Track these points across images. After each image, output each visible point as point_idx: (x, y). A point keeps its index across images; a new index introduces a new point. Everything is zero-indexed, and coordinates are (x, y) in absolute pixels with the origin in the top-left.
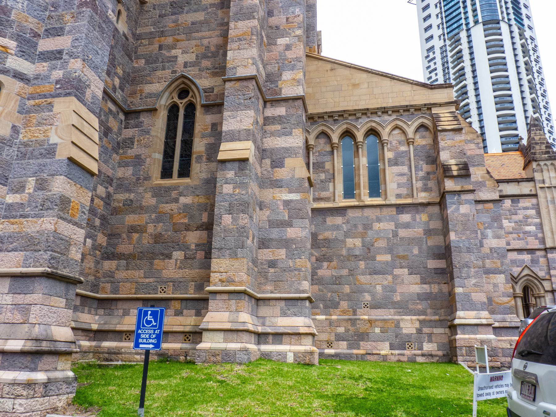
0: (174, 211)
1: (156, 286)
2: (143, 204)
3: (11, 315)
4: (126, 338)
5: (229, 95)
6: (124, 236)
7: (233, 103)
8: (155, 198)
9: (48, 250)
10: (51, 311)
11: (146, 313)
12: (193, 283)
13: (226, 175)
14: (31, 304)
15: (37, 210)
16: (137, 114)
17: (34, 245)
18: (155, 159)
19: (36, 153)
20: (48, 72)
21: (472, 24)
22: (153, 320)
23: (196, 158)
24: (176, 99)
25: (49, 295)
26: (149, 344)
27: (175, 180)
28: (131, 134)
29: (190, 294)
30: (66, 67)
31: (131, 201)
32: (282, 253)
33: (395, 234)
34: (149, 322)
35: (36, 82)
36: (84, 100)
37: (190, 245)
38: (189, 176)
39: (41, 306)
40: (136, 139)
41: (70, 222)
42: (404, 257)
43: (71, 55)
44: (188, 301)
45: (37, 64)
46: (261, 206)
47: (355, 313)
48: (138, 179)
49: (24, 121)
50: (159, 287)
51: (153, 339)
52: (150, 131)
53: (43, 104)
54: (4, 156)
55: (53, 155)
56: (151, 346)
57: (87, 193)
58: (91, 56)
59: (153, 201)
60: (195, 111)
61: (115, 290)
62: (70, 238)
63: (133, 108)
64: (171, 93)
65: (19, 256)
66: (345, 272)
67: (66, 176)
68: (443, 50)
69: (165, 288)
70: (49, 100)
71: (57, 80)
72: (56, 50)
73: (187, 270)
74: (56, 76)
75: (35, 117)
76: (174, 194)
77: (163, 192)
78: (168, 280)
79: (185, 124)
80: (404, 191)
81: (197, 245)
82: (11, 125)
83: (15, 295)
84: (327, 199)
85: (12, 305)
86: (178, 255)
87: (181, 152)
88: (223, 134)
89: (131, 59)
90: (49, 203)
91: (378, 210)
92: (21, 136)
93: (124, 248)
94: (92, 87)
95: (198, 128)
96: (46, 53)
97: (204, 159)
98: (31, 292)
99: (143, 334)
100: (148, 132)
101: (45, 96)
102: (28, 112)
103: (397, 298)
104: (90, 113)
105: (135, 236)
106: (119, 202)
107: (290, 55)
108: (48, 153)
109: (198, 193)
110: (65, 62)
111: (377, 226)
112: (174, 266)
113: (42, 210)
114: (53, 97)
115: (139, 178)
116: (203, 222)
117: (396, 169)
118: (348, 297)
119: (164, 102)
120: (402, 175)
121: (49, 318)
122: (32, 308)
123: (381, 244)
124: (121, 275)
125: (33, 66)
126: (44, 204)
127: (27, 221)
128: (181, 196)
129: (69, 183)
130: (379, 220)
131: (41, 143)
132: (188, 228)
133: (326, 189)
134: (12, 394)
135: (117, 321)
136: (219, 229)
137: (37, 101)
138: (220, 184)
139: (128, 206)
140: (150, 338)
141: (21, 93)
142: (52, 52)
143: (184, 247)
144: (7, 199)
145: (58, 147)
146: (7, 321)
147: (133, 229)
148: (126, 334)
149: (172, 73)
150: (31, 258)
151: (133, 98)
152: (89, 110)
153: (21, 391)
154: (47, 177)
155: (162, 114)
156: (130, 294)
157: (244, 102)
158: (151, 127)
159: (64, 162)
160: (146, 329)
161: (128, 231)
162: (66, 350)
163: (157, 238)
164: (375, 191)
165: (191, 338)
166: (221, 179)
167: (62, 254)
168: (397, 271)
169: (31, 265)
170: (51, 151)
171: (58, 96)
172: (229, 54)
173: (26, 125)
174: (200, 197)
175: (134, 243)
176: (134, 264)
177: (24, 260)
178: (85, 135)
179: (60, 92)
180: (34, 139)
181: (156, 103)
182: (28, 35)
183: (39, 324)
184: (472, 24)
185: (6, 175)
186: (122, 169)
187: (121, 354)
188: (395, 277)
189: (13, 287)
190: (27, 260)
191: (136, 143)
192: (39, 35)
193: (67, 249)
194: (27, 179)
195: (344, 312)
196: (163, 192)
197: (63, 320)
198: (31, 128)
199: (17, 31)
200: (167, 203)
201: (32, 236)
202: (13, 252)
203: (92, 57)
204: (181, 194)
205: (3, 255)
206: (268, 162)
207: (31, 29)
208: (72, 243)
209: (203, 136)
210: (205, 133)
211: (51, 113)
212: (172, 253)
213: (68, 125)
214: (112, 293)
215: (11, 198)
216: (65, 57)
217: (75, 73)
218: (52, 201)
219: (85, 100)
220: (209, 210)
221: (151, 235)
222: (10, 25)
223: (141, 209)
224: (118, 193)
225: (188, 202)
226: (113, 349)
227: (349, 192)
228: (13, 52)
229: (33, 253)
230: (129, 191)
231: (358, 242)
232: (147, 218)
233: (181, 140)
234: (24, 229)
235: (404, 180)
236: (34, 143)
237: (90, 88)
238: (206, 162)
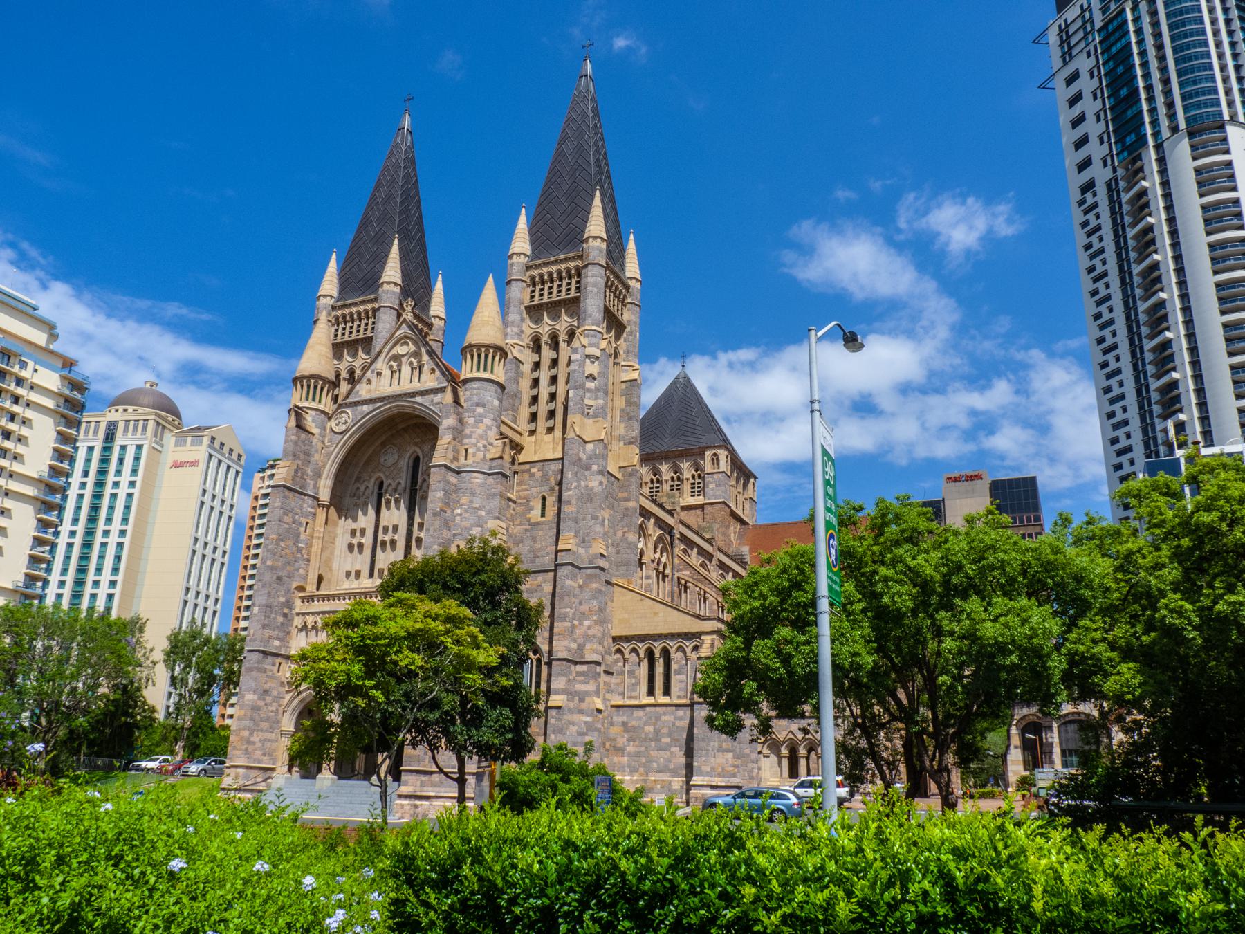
21: (1166, 133)
33: (674, 724)
42: (677, 740)
46: (573, 724)
47: (647, 775)
66: (643, 749)
68: (1112, 187)
80: (682, 694)
84: (635, 698)
91: (664, 708)
103: (672, 766)
107: (590, 633)
111: (663, 718)
117: (678, 677)
118: (644, 765)
120: (682, 682)
123: (665, 731)
130: (665, 714)
133: (635, 691)
164: (667, 692)
168: (673, 749)
184: (1166, 133)
188: (672, 753)
195: (641, 775)
206: (577, 699)
227: (651, 692)
231: (651, 729)
235: (683, 686)
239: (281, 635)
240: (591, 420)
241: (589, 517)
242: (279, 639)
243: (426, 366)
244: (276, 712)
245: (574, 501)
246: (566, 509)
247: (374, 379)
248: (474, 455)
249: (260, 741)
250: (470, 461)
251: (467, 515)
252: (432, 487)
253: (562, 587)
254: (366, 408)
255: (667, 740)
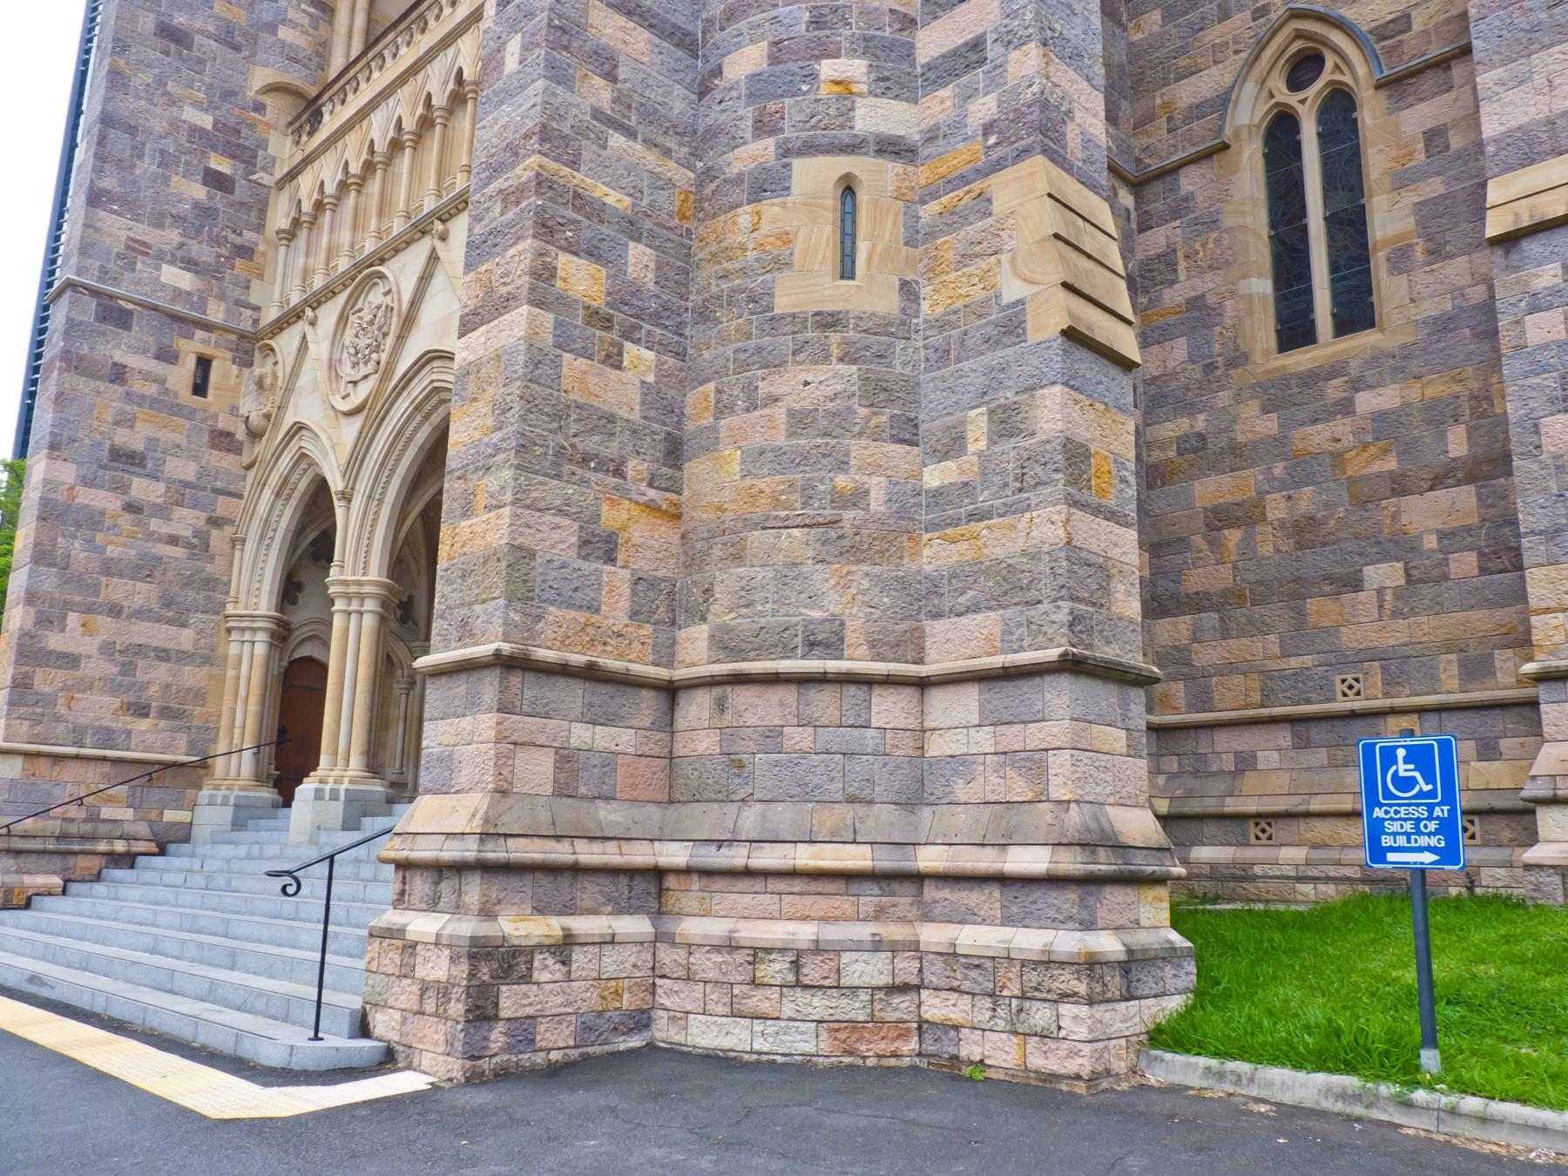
0: (1344, 442)
1: (1326, 678)
2: (1240, 439)
3: (998, 780)
4: (1260, 835)
5: (1485, 11)
6: (1198, 541)
7: (1504, 33)
8: (1274, 416)
9: (1062, 598)
10: (1097, 764)
11: (1389, 756)
12: (1453, 657)
13: (1527, 284)
14: (1046, 750)
15: (1009, 493)
16: (1170, 179)
17: (1022, 588)
18: (1250, 296)
19: (974, 340)
20: (958, 111)
22: (1417, 775)
23: (1388, 259)
24: (1284, 96)
25: (1086, 721)
26: (1421, 850)
27: (1327, 345)
28: (1162, 241)
29: (1449, 692)
30: (1002, 81)
31: (1201, 437)
34: (1405, 784)
35: (930, 149)
36: (1065, 159)
37: (1420, 537)
38: (1372, 325)
39: (1073, 752)
40: (1180, 254)
41: (1097, 511)
43: (1010, 41)
44: (1445, 715)
45: (924, 100)
48: (1210, 368)
49: (925, 262)
50: (1338, 679)
51: (1429, 834)
52: (1220, 217)
53: (963, 202)
54: (899, 369)
55: (1018, 336)
56: (1428, 858)
57: (1123, 424)
58: (1058, 27)
59: (1269, 425)
60: (1354, 109)
61: (1202, 700)
62: (1107, 559)
63: (1154, 164)
64: (1264, 82)
65: (987, 623)
67: (1066, 384)
69: (1357, 680)
70: (976, 186)
71: (984, 125)
72: (966, 44)
73: (1424, 619)
74: (979, 115)
75: (950, 245)
76: (1334, 390)
77: (1297, 390)
78: (1361, 656)
79: (1327, 162)
81: (1442, 536)
82: (897, 283)
83: (999, 728)
85: (996, 753)
86: (1384, 575)
87: (1330, 255)
88: (1490, 149)
89: (1119, 23)
90: (1038, 469)
92: (925, 306)
93: (1204, 577)
94: (1078, 115)
95: (1376, 162)
96: (940, 61)
97: (1419, 254)
98: (1039, 716)
99: (1391, 819)
100: (1213, 223)
101: (964, 180)
102: (931, 235)
104: (1086, 191)
105: (1233, 537)
106: (1163, 448)
108: (1005, 333)
109: (1416, 370)
110: (995, 68)
112: (1376, 611)
113: (1020, 490)
114: (984, 173)
115: (1211, 364)
116: (1454, 459)
119: (1249, 113)
121: (1098, 785)
122: (1051, 759)
124: (1208, 655)
125: (914, 109)
126: (1023, 474)
127: (989, 528)
128: (1357, 390)
129: (1076, 402)
131: (979, 310)
132: (1399, 486)
134: (1049, 991)
135: (1223, 786)
136: (1535, 467)
137: (944, 199)
138: (1511, 319)
139: (1195, 453)
140: (1419, 833)
141: (903, 190)
142: (955, 53)
143: (1399, 546)
144: (926, 478)
145: (1029, 307)
146: (993, 798)
147: (1220, 518)
148: (1257, 824)
149: (1254, 19)
150: (1019, 625)
151: (1149, 137)
152: (1082, 183)
153: (1072, 983)
154: (1016, 399)
155: (1246, 153)
156: (1247, 706)
157: (1551, 16)
158: (1218, 205)
159: (1055, 344)
160: (1400, 805)
161: (1207, 525)
162: (1154, 872)
163: (1303, 531)
165: (1476, 829)
166: (1513, 300)
167: (1094, 604)
169: (1025, 644)
170: (1012, 325)
171: (998, 166)
173: (933, 272)
174: (1425, 379)
175: (1233, 558)
176: (1243, 620)
177: (1003, 633)
178: (1090, 257)
179: (1000, 154)
180: (959, 304)
181: (1221, 129)
182: (888, 30)
183: (1077, 802)
185: (913, 415)
186: (1157, 348)
187: (1254, 878)
189: (990, 707)
190: (1012, 633)
191: (1182, 265)
192: (913, 21)
193: (1105, 589)
194: (965, 416)
196: (1297, 390)
197: (1128, 789)
198: (945, 278)
199: (860, 28)
200: (1315, 421)
201: (1009, 566)
202: (971, 616)
203: (1062, 26)
204: (1358, 384)
205: (948, 627)
207: (891, 10)
208: (1113, 571)
209: (1401, 181)
210: (1406, 171)
211: (990, 220)
212: (1361, 571)
213: (1043, 240)
214: (1193, 708)
215: (936, 473)
216: (993, 51)
217: (1031, 86)
218: (1043, 460)
219: (1068, 156)
220: (1467, 418)
221: (1283, 526)
222: (843, 19)
223: (1237, 455)
224: (1156, 423)
225: (1385, 407)
226: (1227, 866)
228: (863, 88)
229: (1021, 612)
230: (1188, 408)
232: (1260, 477)
233: (1326, 219)
234: (986, 551)
236: (961, 314)
237: (1073, 119)
238: (1429, 264)
239: (202, 251)
242: (190, 264)
244: (200, 546)
249: (107, 650)
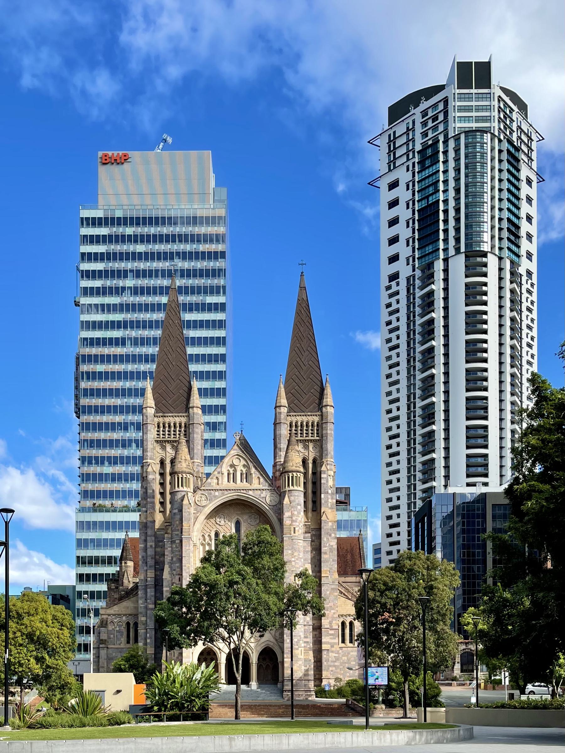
32: (334, 668)
111: (351, 653)
123: (352, 659)
130: (352, 652)
172: (323, 621)
227: (343, 641)
231: (346, 658)
240: (330, 510)
241: (331, 560)
243: (254, 475)
245: (328, 553)
246: (324, 556)
247: (220, 478)
248: (298, 531)
250: (297, 534)
251: (298, 561)
252: (285, 548)
253: (325, 595)
254: (217, 493)
255: (354, 663)
